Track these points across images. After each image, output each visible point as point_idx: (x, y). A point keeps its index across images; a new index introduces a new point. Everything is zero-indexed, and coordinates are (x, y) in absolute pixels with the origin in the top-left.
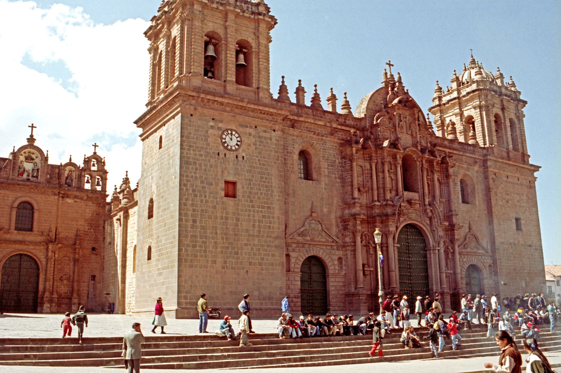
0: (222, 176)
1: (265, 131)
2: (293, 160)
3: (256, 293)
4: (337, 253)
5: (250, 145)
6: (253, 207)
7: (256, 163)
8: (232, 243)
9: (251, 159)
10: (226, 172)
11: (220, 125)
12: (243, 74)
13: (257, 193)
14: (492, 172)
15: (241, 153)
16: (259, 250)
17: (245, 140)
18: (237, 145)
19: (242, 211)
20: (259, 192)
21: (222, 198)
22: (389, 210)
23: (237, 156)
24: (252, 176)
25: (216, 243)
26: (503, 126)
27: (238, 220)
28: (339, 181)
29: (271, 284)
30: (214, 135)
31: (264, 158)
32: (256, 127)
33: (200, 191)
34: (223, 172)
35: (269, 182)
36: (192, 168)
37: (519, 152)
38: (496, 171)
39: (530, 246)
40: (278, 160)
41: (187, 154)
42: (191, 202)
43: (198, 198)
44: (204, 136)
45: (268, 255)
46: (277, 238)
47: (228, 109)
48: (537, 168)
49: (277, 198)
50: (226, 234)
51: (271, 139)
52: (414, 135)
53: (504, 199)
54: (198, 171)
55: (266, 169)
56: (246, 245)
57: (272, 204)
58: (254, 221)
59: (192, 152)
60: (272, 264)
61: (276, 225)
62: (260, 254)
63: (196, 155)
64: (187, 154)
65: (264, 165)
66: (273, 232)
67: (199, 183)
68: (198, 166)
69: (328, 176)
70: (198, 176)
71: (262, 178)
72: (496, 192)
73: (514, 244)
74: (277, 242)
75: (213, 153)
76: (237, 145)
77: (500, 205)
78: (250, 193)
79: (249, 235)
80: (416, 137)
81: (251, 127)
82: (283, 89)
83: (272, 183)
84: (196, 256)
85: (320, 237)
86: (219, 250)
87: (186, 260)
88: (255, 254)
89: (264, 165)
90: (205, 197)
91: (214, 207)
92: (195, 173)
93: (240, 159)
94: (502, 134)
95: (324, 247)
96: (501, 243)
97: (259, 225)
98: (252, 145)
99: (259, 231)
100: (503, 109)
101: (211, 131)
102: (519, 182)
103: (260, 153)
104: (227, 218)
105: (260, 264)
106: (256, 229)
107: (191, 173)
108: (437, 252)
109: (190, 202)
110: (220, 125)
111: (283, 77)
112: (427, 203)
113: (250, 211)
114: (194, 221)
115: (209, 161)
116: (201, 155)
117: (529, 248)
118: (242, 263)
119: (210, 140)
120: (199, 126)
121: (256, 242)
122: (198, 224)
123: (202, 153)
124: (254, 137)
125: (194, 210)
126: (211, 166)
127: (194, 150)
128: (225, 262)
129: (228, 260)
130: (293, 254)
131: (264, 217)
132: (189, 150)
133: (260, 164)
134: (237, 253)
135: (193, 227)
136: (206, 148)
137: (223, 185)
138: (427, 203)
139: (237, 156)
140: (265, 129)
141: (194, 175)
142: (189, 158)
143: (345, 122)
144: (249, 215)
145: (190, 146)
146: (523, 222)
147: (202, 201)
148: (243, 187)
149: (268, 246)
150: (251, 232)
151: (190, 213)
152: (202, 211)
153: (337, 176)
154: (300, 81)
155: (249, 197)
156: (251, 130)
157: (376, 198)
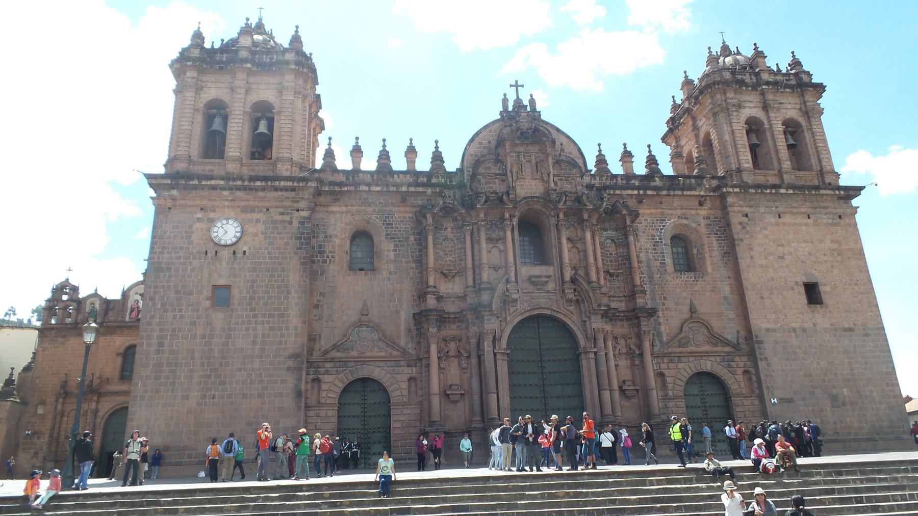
1: (282, 214)
2: (333, 247)
4: (407, 370)
5: (256, 235)
6: (255, 316)
7: (264, 258)
11: (212, 215)
12: (262, 146)
14: (739, 212)
17: (251, 229)
19: (237, 323)
20: (266, 296)
21: (207, 309)
22: (485, 297)
23: (234, 253)
24: (258, 276)
25: (191, 371)
26: (768, 134)
27: (229, 336)
28: (414, 265)
30: (202, 229)
31: (278, 248)
32: (268, 210)
34: (210, 274)
35: (283, 281)
36: (165, 276)
37: (812, 170)
38: (746, 210)
39: (850, 330)
40: (301, 249)
41: (158, 258)
42: (157, 320)
43: (170, 315)
44: (186, 232)
46: (291, 357)
47: (226, 193)
48: (857, 190)
49: (296, 300)
50: (209, 358)
51: (291, 223)
52: (546, 179)
53: (771, 254)
54: (173, 279)
55: (280, 263)
56: (239, 370)
57: (286, 309)
58: (255, 336)
59: (166, 255)
63: (171, 258)
64: (158, 258)
66: (285, 349)
67: (173, 295)
69: (395, 261)
70: (172, 284)
71: (271, 276)
72: (750, 245)
73: (804, 330)
74: (291, 363)
75: (199, 252)
77: (761, 266)
78: (252, 298)
80: (548, 182)
81: (261, 212)
83: (288, 281)
85: (376, 350)
86: (194, 381)
90: (181, 310)
91: (194, 324)
92: (168, 281)
93: (239, 255)
94: (768, 148)
95: (383, 364)
96: (768, 330)
98: (260, 234)
99: (263, 350)
100: (765, 107)
101: (197, 225)
102: (809, 221)
103: (271, 244)
104: (211, 337)
105: (260, 396)
108: (592, 356)
112: (567, 277)
113: (249, 323)
114: (161, 345)
115: (191, 263)
116: (179, 258)
117: (847, 334)
118: (230, 396)
119: (194, 236)
123: (181, 254)
125: (161, 330)
126: (193, 270)
127: (168, 253)
128: (204, 397)
130: (327, 378)
131: (271, 329)
132: (162, 253)
133: (271, 258)
134: (223, 383)
135: (158, 352)
136: (188, 248)
137: (207, 292)
138: (567, 277)
139: (234, 253)
140: (282, 210)
145: (163, 248)
146: (824, 289)
147: (175, 317)
148: (240, 292)
150: (249, 352)
151: (155, 334)
152: (174, 330)
153: (411, 259)
154: (357, 138)
155: (250, 304)
156: (261, 215)
157: (471, 283)
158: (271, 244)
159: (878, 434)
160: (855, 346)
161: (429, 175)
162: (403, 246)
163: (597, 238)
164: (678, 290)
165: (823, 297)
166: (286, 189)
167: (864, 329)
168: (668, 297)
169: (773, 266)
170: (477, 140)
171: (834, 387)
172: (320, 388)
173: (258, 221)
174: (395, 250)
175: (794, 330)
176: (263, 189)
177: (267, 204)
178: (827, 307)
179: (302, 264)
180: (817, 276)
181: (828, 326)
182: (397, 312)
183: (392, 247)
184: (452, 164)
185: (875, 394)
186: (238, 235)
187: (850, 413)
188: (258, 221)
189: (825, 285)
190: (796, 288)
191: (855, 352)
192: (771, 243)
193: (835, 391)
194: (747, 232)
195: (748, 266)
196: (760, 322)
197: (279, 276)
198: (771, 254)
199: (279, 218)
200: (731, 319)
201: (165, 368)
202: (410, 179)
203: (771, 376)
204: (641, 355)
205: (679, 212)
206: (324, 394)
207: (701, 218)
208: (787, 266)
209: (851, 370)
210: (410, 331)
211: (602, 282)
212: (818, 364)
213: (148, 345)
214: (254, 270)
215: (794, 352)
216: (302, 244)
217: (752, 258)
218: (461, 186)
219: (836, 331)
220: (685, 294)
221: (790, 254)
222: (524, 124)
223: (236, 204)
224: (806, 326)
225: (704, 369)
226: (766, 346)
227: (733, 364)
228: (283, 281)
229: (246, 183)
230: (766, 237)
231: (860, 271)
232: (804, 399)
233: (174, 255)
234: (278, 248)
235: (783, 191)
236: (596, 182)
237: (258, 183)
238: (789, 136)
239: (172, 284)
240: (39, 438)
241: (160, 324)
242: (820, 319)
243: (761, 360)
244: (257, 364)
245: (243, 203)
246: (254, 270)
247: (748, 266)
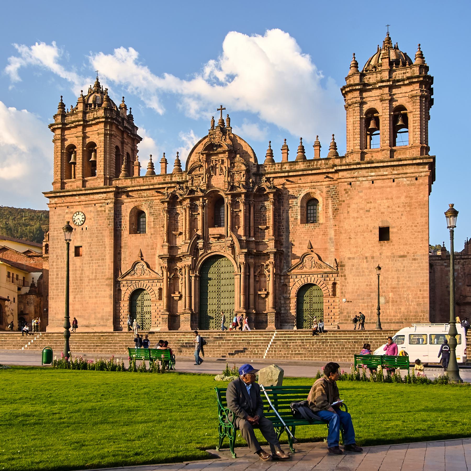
0: (73, 244)
1: (101, 206)
3: (93, 316)
4: (158, 284)
5: (91, 219)
6: (92, 260)
8: (79, 286)
9: (92, 228)
10: (75, 240)
11: (72, 210)
13: (94, 251)
15: (85, 226)
16: (96, 288)
18: (82, 221)
19: (85, 264)
24: (92, 240)
27: (82, 270)
29: (103, 309)
31: (100, 225)
33: (60, 256)
35: (103, 242)
40: (109, 225)
45: (102, 291)
46: (107, 279)
47: (77, 198)
51: (105, 211)
53: (361, 209)
55: (101, 233)
56: (87, 286)
57: (105, 256)
58: (93, 270)
59: (56, 232)
60: (104, 297)
61: (107, 271)
62: (96, 291)
65: (100, 230)
66: (105, 276)
68: (59, 241)
69: (154, 228)
73: (373, 258)
74: (107, 282)
76: (82, 221)
77: (354, 218)
78: (90, 251)
79: (89, 280)
81: (92, 206)
83: (105, 242)
84: (58, 295)
87: (53, 298)
88: (92, 291)
89: (100, 230)
92: (58, 245)
93: (84, 229)
96: (349, 258)
97: (96, 272)
98: (93, 219)
99: (96, 276)
105: (96, 297)
106: (94, 274)
107: (55, 245)
109: (55, 264)
110: (72, 210)
113: (90, 263)
114: (57, 275)
117: (400, 259)
120: (59, 215)
121: (94, 283)
122: (59, 276)
125: (57, 268)
127: (57, 231)
128: (75, 298)
129: (77, 296)
131: (99, 266)
132: (54, 231)
133: (97, 230)
134: (81, 291)
135: (57, 278)
141: (57, 246)
142: (54, 236)
143: (171, 179)
144: (89, 267)
145: (55, 229)
147: (61, 262)
149: (102, 285)
150: (91, 277)
151: (55, 270)
156: (92, 208)
158: (97, 223)
159: (406, 319)
160: (404, 267)
162: (157, 219)
164: (302, 236)
165: (391, 235)
167: (414, 256)
168: (296, 240)
169: (361, 217)
170: (195, 151)
173: (91, 211)
174: (154, 221)
175: (366, 258)
177: (94, 202)
178: (392, 242)
181: (389, 254)
182: (154, 255)
183: (153, 220)
185: (410, 296)
186: (83, 220)
187: (390, 307)
191: (403, 270)
192: (363, 202)
194: (348, 196)
195: (345, 218)
196: (345, 254)
197: (101, 239)
198: (361, 209)
199: (99, 209)
200: (332, 252)
201: (60, 285)
202: (161, 180)
203: (346, 286)
205: (309, 184)
207: (324, 187)
208: (371, 216)
209: (398, 282)
211: (252, 234)
213: (53, 275)
214: (90, 237)
215: (363, 272)
217: (348, 212)
219: (394, 257)
220: (306, 238)
223: (82, 203)
224: (375, 255)
226: (346, 268)
227: (328, 279)
228: (103, 242)
233: (59, 232)
234: (100, 225)
239: (59, 246)
241: (57, 265)
243: (342, 276)
244: (94, 283)
245: (84, 203)
246: (90, 237)
247: (345, 218)
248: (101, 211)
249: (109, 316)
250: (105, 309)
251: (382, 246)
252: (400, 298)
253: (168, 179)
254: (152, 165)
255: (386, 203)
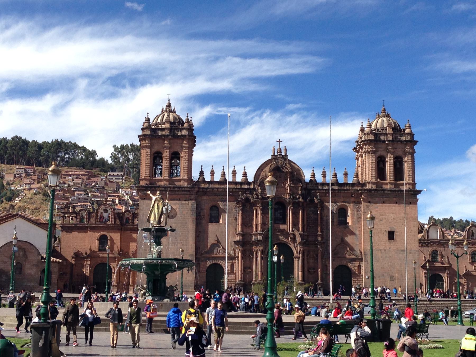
48: (419, 192)
51: (188, 204)
57: (188, 238)
66: (188, 253)
73: (385, 250)
82: (202, 173)
111: (202, 166)
113: (175, 243)
117: (402, 252)
124: (179, 204)
144: (174, 245)
161: (241, 183)
163: (305, 212)
166: (186, 191)
171: (392, 273)
172: (200, 266)
175: (381, 250)
176: (178, 191)
179: (193, 221)
180: (395, 228)
184: (251, 178)
188: (176, 204)
189: (398, 232)
190: (385, 233)
193: (392, 275)
204: (317, 258)
206: (201, 269)
208: (383, 224)
210: (232, 246)
212: (388, 264)
215: (379, 259)
216: (192, 213)
218: (254, 189)
221: (385, 219)
222: (281, 162)
225: (342, 264)
227: (355, 262)
229: (172, 189)
230: (377, 211)
231: (414, 227)
232: (379, 277)
235: (386, 192)
236: (309, 187)
237: (176, 189)
238: (398, 163)
240: (66, 275)
242: (392, 246)
248: (186, 204)
249: (191, 283)
250: (188, 278)
251: (390, 243)
252: (402, 277)
253: (238, 186)
254: (224, 174)
255: (392, 216)
